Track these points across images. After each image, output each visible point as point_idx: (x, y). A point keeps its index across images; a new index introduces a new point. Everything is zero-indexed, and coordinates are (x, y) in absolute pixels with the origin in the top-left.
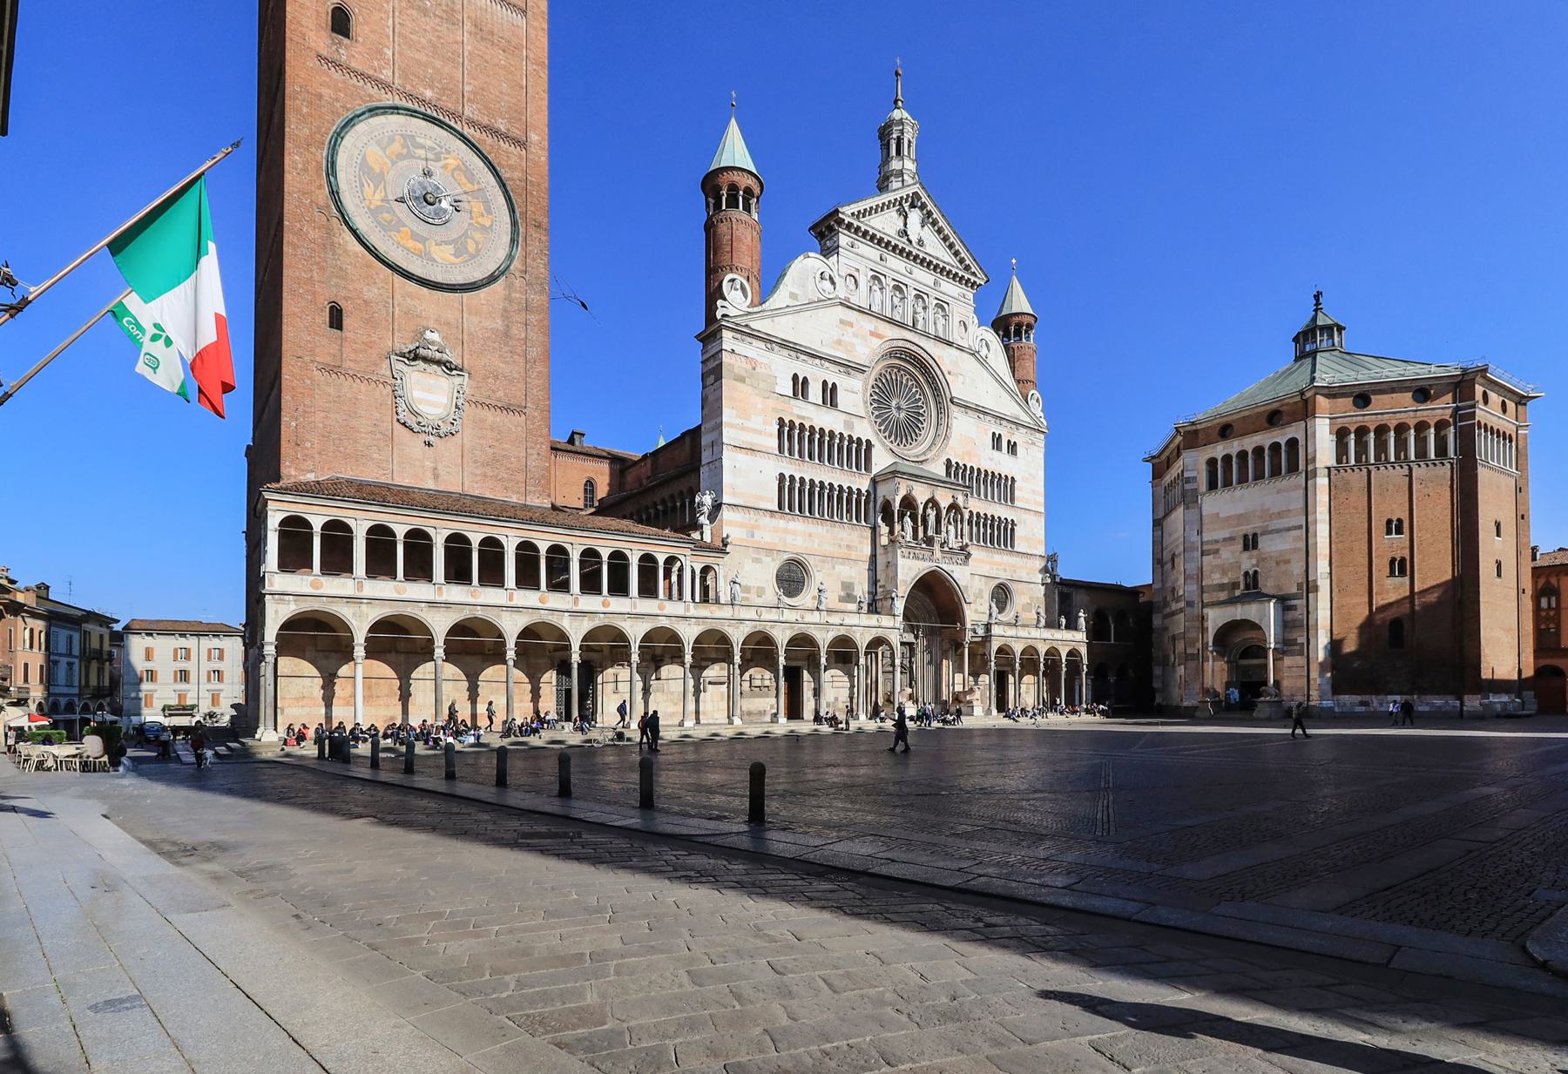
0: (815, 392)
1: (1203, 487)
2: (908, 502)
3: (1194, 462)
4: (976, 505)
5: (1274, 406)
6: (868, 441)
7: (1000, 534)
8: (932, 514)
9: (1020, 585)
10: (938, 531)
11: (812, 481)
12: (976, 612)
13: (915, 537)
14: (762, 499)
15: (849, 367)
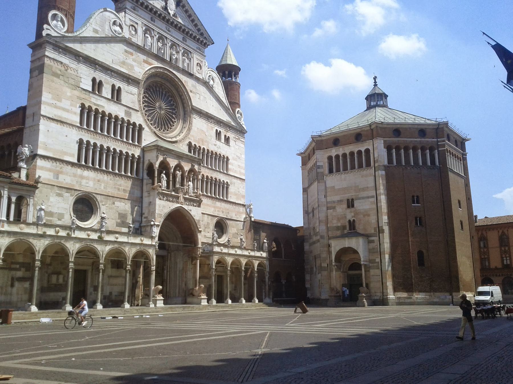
0: (107, 92)
1: (327, 171)
2: (164, 166)
3: (321, 158)
4: (205, 172)
5: (359, 131)
6: (140, 125)
7: (219, 190)
8: (179, 173)
10: (182, 184)
11: (102, 146)
12: (205, 236)
13: (168, 187)
14: (66, 154)
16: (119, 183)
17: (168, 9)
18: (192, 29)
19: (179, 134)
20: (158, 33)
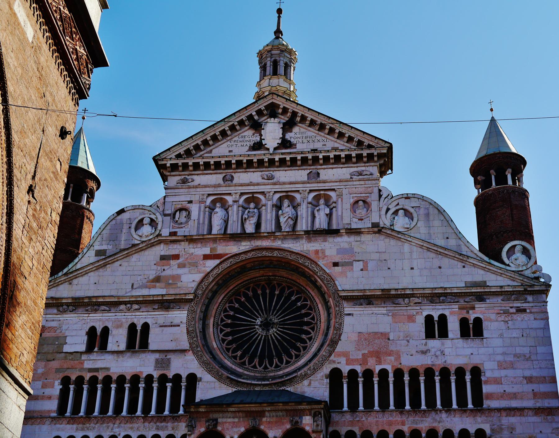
0: (118, 339)
17: (264, 142)
18: (336, 145)
19: (310, 361)
20: (242, 194)
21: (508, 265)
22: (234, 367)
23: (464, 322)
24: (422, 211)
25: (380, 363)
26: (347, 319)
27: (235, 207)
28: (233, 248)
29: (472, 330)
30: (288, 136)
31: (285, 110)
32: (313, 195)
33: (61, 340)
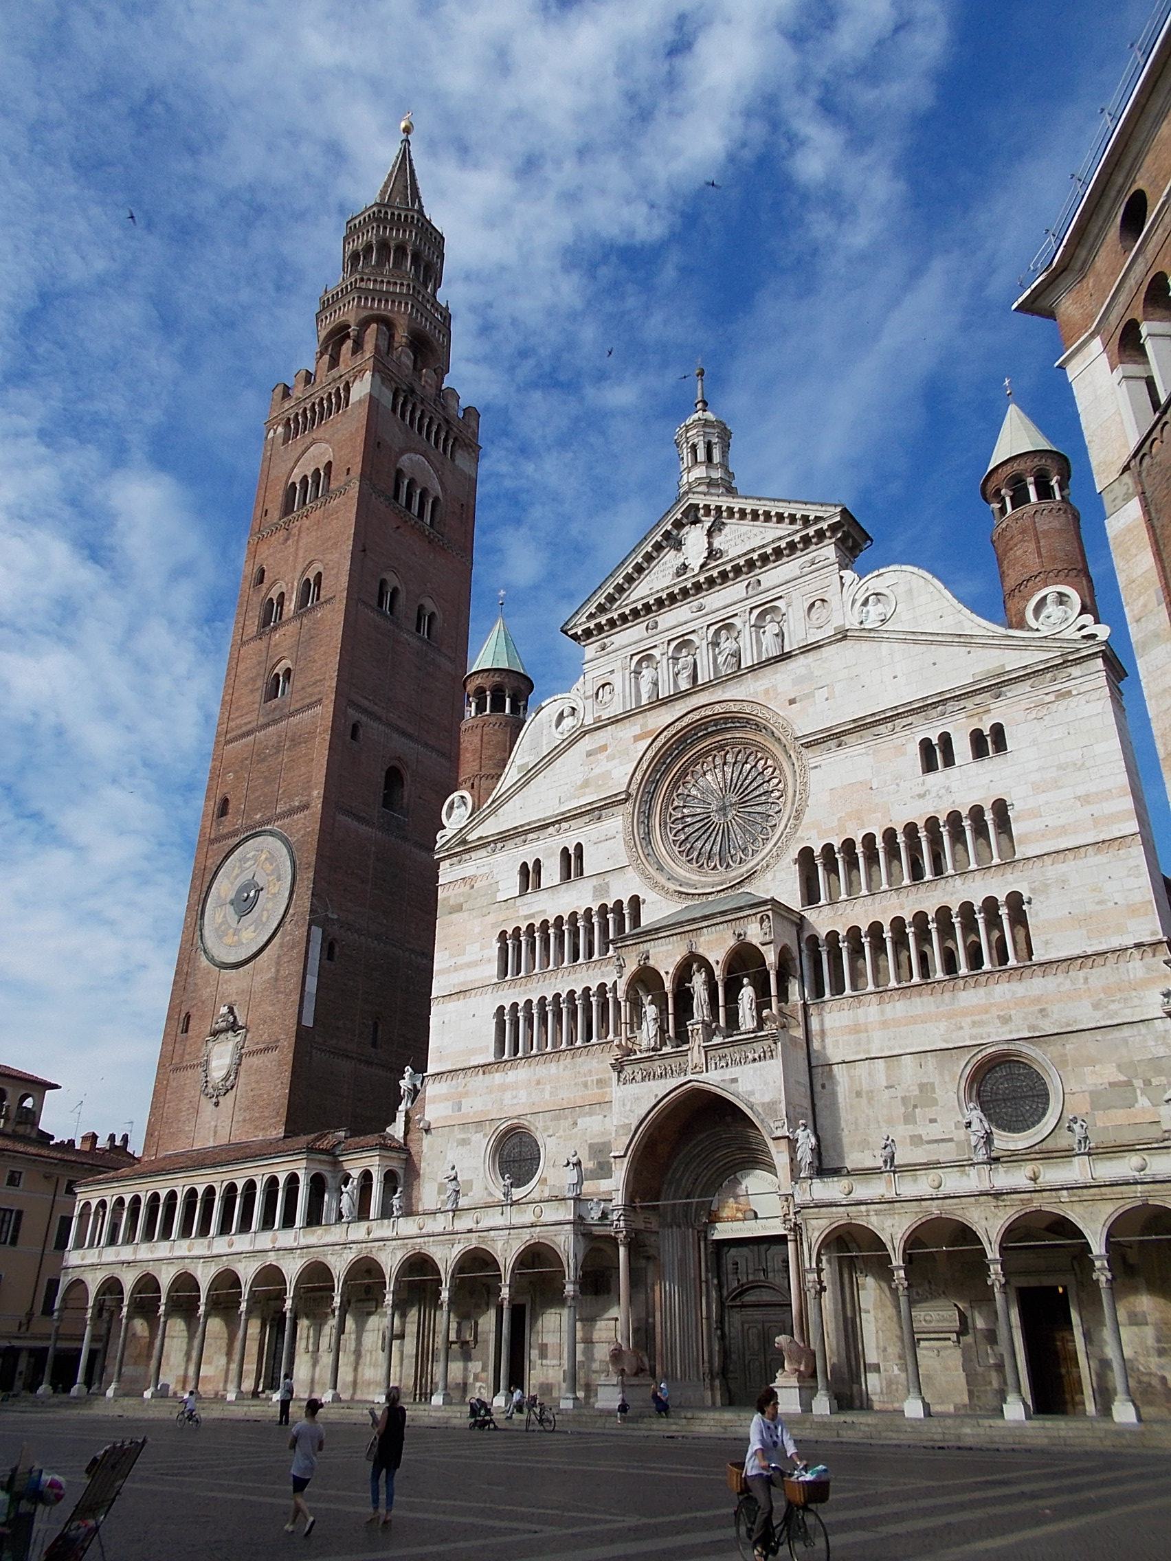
0: (551, 873)
7: (988, 939)
9: (1071, 1046)
14: (473, 1052)
15: (595, 812)
16: (585, 1069)
21: (1037, 630)
22: (688, 875)
23: (977, 738)
24: (901, 589)
25: (863, 828)
26: (813, 776)
27: (665, 661)
28: (663, 717)
29: (988, 743)
30: (716, 544)
31: (707, 507)
32: (756, 612)
33: (494, 887)
